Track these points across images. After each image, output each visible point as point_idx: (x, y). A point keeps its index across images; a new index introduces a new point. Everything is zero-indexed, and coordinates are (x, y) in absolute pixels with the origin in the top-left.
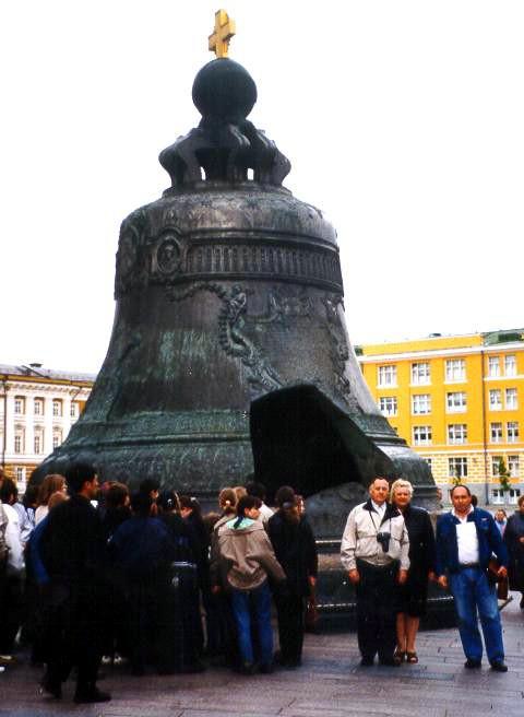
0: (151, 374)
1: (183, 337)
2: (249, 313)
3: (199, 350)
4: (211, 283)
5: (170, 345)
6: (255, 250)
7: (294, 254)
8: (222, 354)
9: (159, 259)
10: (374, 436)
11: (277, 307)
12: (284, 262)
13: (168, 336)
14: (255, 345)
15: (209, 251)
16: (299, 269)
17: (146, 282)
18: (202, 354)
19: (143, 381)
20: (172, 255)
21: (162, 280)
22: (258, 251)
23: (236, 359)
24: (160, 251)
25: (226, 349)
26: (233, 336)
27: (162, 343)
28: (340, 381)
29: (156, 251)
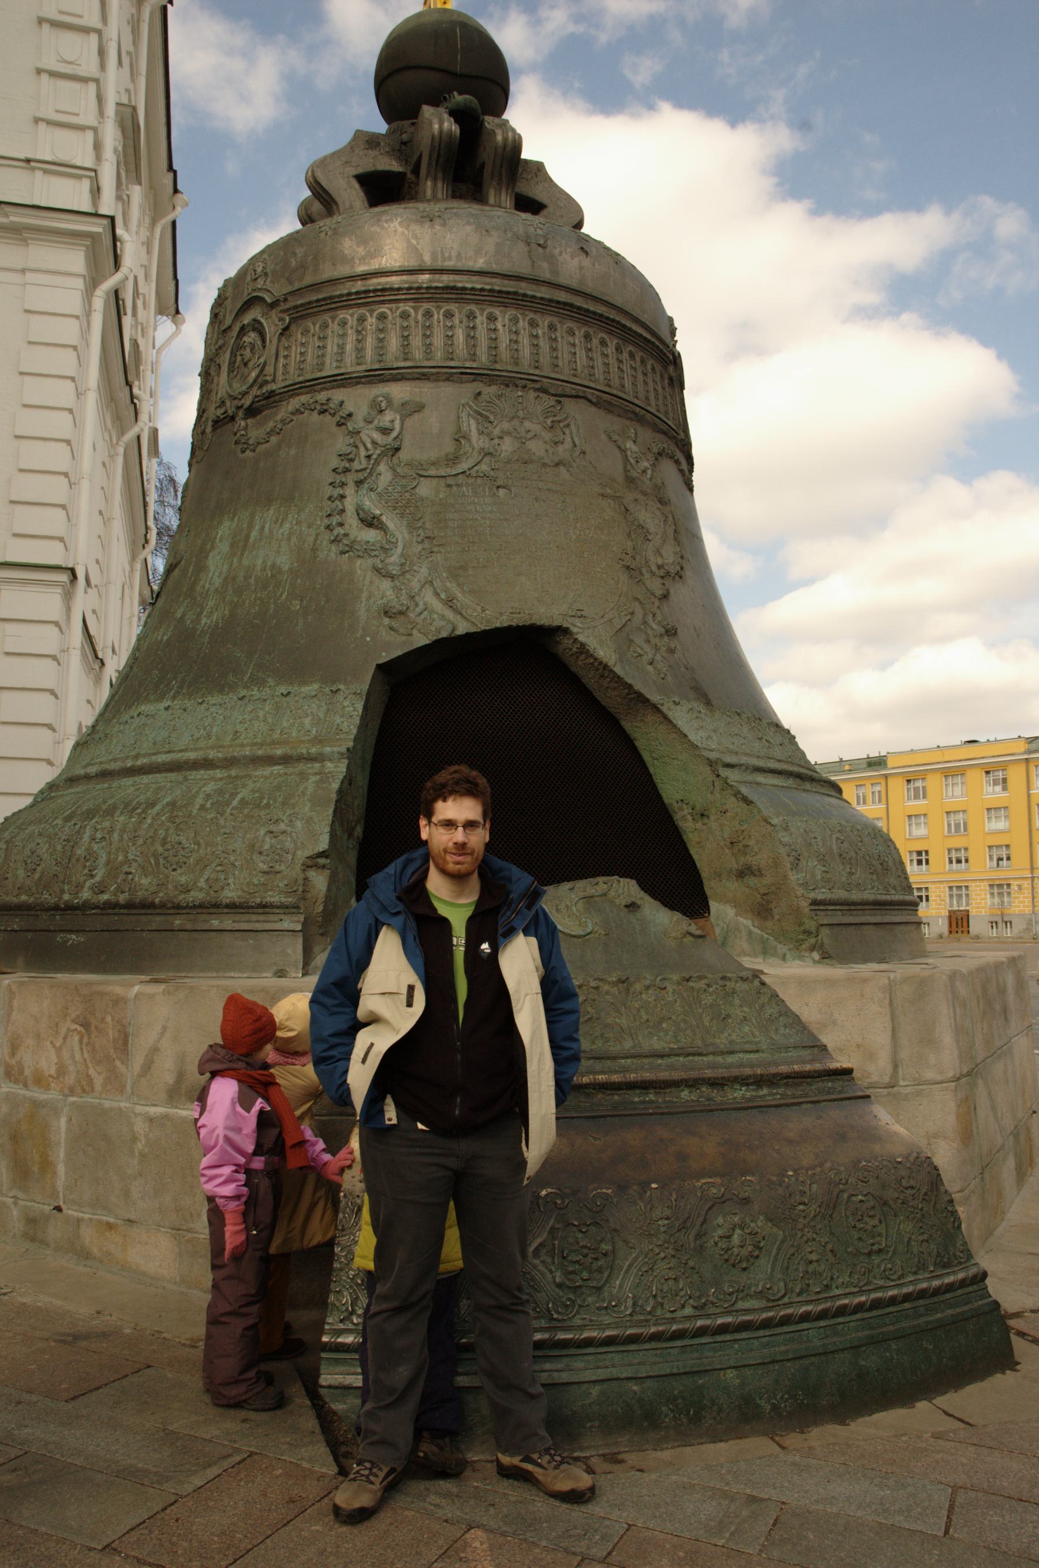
0: (183, 616)
1: (250, 527)
2: (403, 455)
3: (278, 552)
4: (322, 397)
5: (224, 547)
6: (428, 314)
7: (533, 324)
8: (329, 553)
9: (232, 363)
10: (729, 759)
11: (477, 441)
12: (504, 339)
13: (225, 529)
14: (411, 528)
15: (325, 326)
16: (545, 359)
17: (209, 429)
18: (284, 561)
19: (165, 638)
20: (251, 350)
21: (230, 413)
22: (438, 316)
23: (359, 562)
24: (233, 355)
25: (336, 541)
26: (359, 509)
27: (213, 548)
28: (645, 623)
29: (228, 355)
